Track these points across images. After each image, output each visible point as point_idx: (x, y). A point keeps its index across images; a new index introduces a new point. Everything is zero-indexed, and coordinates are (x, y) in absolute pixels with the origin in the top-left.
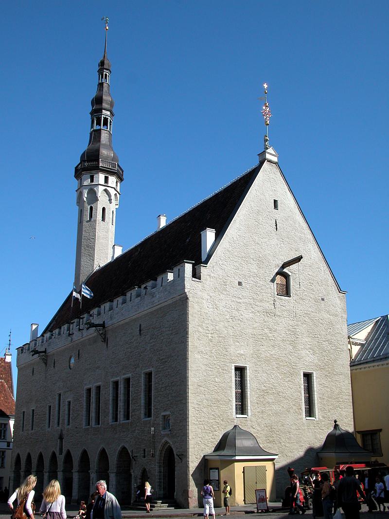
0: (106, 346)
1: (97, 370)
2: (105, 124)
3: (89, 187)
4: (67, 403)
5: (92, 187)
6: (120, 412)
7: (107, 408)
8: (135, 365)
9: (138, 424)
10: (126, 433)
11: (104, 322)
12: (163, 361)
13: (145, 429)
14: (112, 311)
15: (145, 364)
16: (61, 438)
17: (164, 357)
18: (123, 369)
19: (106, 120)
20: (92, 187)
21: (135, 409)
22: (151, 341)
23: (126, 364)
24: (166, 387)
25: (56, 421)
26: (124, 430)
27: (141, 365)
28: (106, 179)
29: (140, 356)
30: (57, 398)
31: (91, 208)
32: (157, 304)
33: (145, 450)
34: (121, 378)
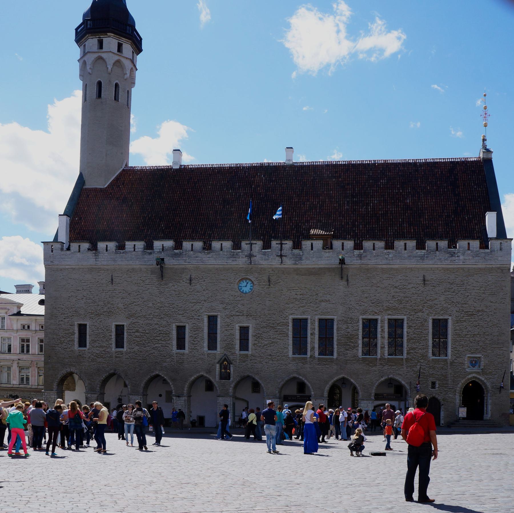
0: (346, 283)
3: (117, 58)
4: (238, 328)
6: (383, 348)
7: (352, 342)
8: (415, 310)
9: (422, 361)
10: (394, 367)
12: (470, 313)
13: (437, 366)
14: (362, 251)
16: (225, 363)
17: (471, 310)
18: (387, 310)
21: (417, 348)
22: (448, 293)
24: (474, 335)
25: (206, 344)
26: (392, 364)
30: (206, 320)
33: (433, 384)
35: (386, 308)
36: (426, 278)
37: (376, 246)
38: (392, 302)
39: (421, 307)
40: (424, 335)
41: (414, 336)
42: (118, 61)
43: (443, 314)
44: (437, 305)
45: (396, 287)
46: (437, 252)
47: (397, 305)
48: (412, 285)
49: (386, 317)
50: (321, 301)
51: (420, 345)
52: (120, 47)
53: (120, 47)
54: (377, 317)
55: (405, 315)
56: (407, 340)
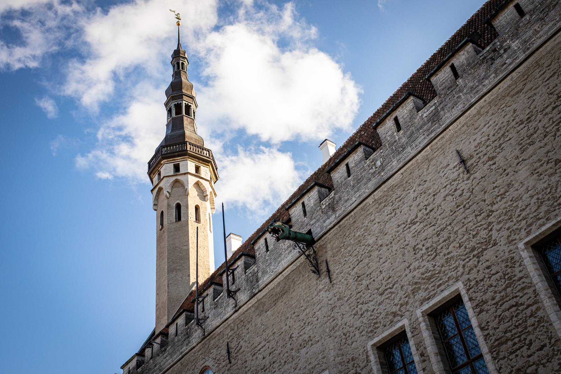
1: (303, 351)
2: (188, 112)
5: (179, 178)
8: (473, 249)
11: (310, 232)
15: (524, 219)
18: (414, 292)
19: (188, 107)
20: (179, 178)
23: (427, 271)
27: (506, 233)
28: (197, 169)
29: (488, 216)
31: (178, 207)
32: (522, 57)
34: (414, 319)
35: (410, 288)
36: (465, 155)
37: (351, 165)
38: (416, 264)
39: (483, 234)
40: (528, 312)
41: (503, 327)
42: (177, 181)
43: (547, 212)
44: (520, 198)
45: (413, 223)
46: (460, 81)
47: (430, 266)
48: (443, 194)
49: (419, 313)
50: (298, 351)
51: (533, 348)
52: (177, 168)
53: (177, 168)
54: (400, 324)
55: (457, 280)
56: (491, 352)
